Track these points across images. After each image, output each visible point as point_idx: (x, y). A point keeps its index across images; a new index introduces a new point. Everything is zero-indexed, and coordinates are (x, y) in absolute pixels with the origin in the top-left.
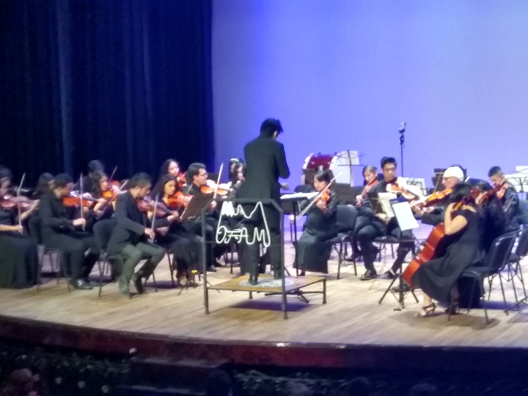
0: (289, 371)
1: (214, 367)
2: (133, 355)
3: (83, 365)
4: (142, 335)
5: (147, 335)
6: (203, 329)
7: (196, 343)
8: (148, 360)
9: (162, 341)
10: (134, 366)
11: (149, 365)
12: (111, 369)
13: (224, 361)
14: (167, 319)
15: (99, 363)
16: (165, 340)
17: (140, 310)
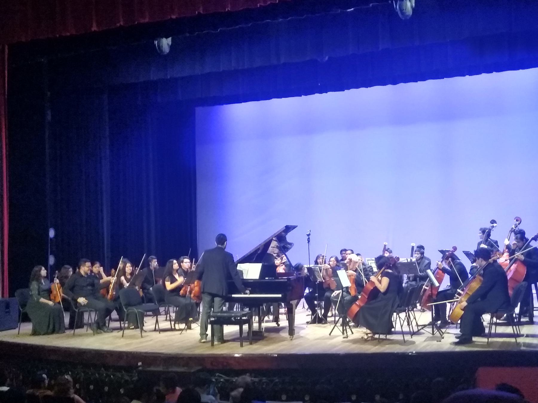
0: (243, 372)
1: (192, 371)
2: (140, 366)
3: (108, 376)
4: (146, 353)
5: (149, 353)
6: (187, 349)
7: (181, 356)
8: (149, 369)
9: (160, 357)
10: (140, 372)
11: (150, 371)
12: (127, 378)
13: (200, 368)
14: (164, 346)
15: (119, 375)
16: (162, 356)
17: (147, 341)
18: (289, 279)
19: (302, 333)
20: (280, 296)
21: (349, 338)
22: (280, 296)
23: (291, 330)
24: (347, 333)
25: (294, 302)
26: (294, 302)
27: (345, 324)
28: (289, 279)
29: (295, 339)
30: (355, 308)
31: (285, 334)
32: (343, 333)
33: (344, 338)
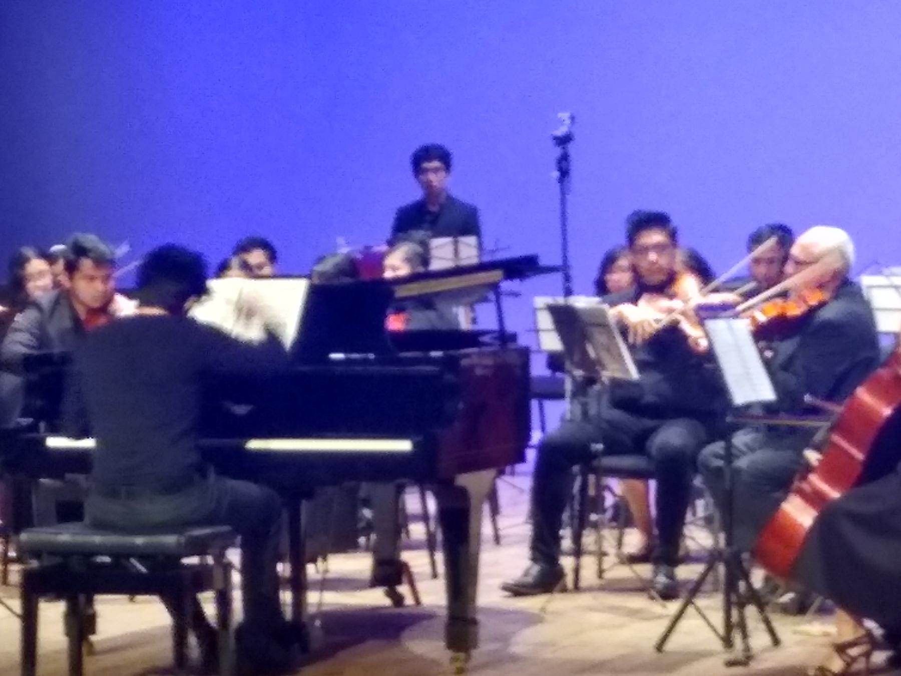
18: (450, 364)
19: (525, 641)
20: (404, 446)
21: (755, 666)
22: (404, 446)
23: (461, 624)
24: (745, 636)
25: (473, 482)
26: (473, 482)
27: (737, 597)
28: (450, 364)
29: (485, 666)
30: (799, 514)
31: (428, 647)
32: (728, 641)
33: (731, 664)
